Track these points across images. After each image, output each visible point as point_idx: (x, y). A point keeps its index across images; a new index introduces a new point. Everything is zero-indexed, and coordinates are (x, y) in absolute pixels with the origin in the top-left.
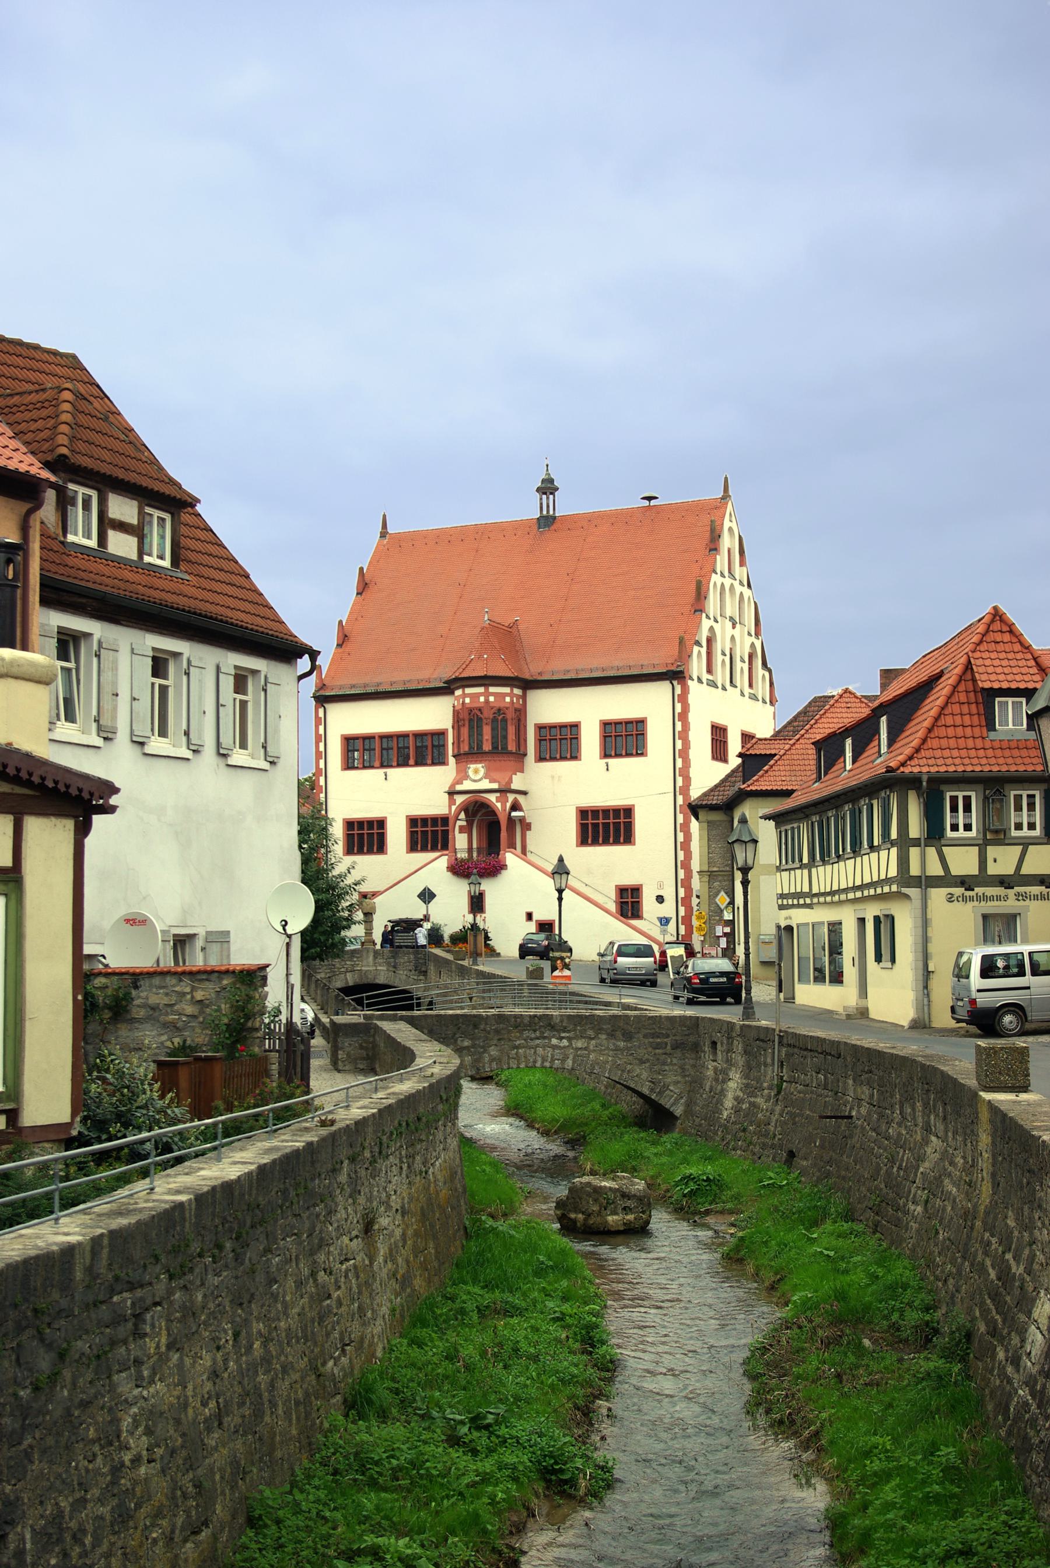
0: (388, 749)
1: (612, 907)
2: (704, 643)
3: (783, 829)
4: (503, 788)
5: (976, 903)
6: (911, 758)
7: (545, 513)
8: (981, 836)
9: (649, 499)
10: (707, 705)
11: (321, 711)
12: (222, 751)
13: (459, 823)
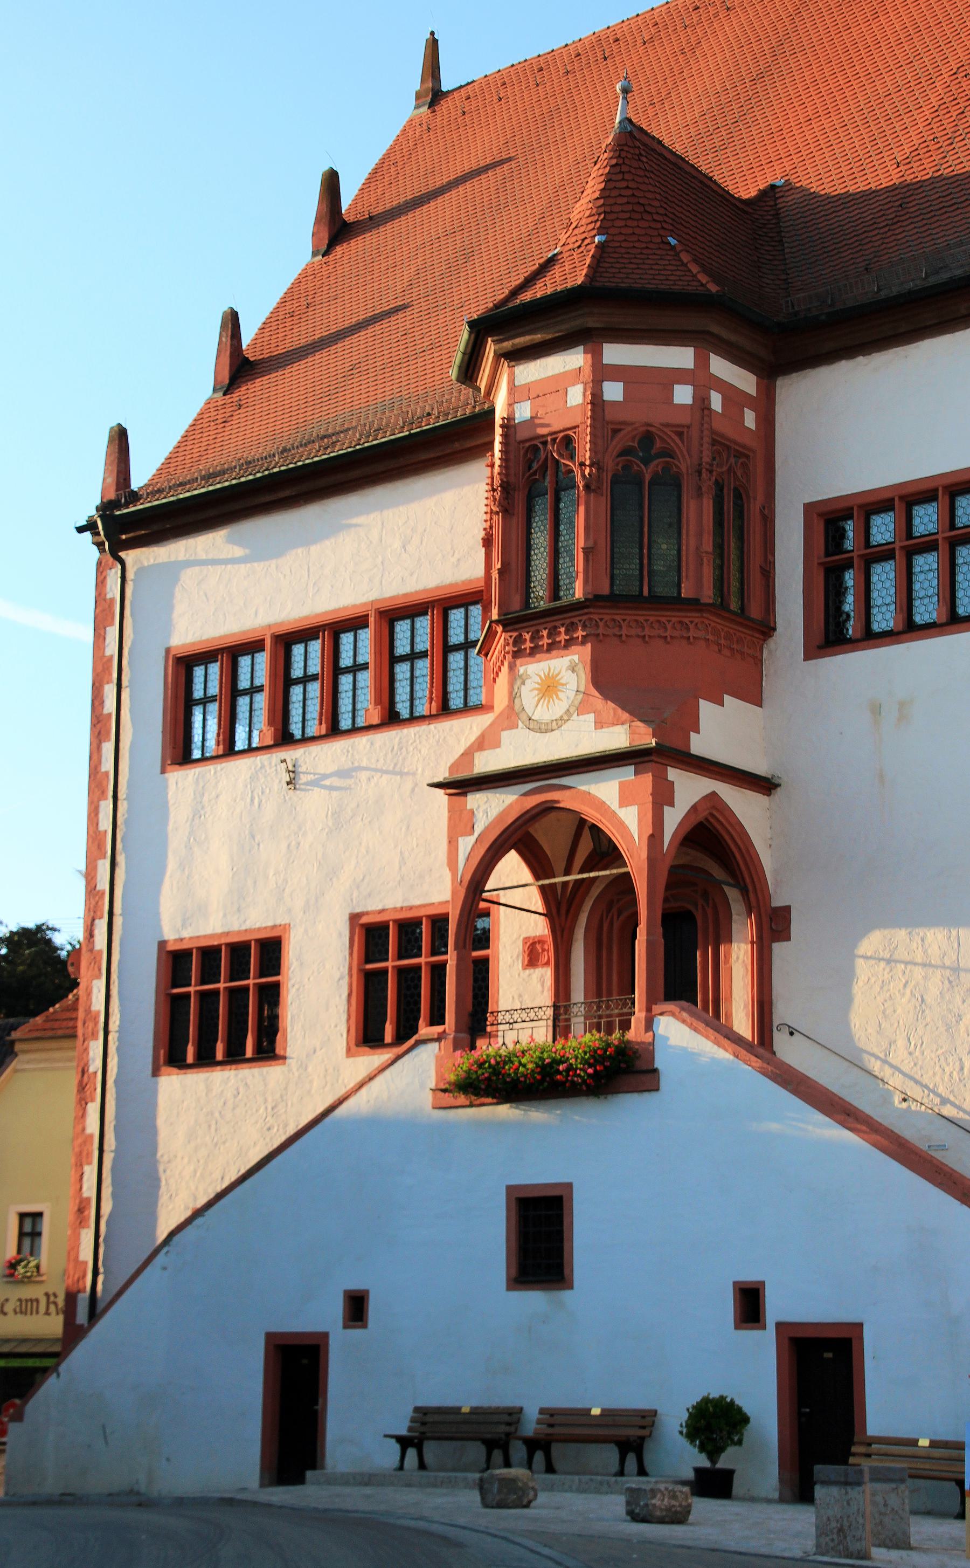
11: (114, 576)
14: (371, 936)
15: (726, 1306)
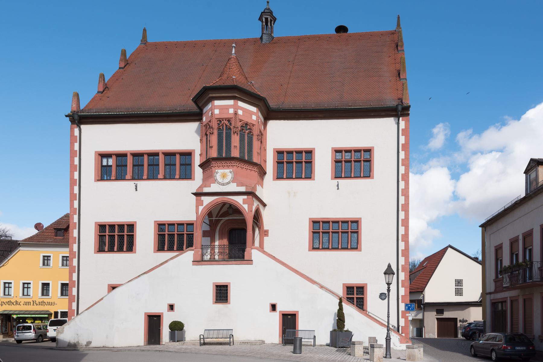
4: (250, 190)
14: (161, 226)
15: (269, 307)
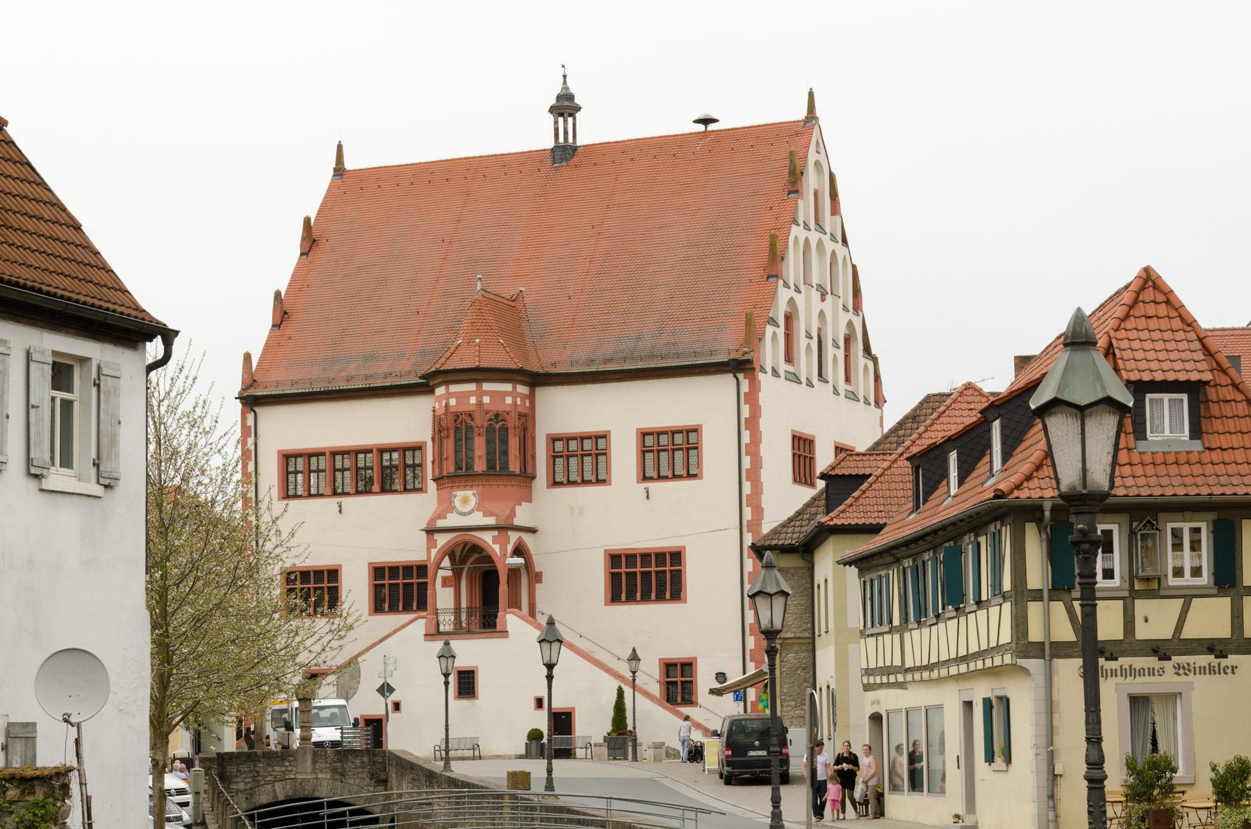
0: (343, 470)
1: (656, 689)
2: (781, 321)
3: (867, 578)
4: (502, 523)
5: (1120, 679)
6: (1029, 478)
7: (561, 140)
8: (1127, 585)
9: (706, 121)
10: (787, 406)
11: (250, 416)
12: (33, 471)
13: (441, 573)
15: (532, 704)
